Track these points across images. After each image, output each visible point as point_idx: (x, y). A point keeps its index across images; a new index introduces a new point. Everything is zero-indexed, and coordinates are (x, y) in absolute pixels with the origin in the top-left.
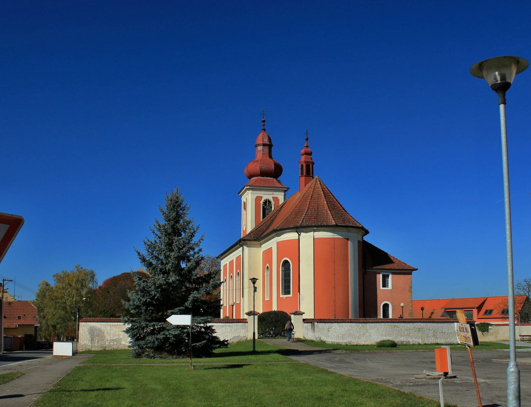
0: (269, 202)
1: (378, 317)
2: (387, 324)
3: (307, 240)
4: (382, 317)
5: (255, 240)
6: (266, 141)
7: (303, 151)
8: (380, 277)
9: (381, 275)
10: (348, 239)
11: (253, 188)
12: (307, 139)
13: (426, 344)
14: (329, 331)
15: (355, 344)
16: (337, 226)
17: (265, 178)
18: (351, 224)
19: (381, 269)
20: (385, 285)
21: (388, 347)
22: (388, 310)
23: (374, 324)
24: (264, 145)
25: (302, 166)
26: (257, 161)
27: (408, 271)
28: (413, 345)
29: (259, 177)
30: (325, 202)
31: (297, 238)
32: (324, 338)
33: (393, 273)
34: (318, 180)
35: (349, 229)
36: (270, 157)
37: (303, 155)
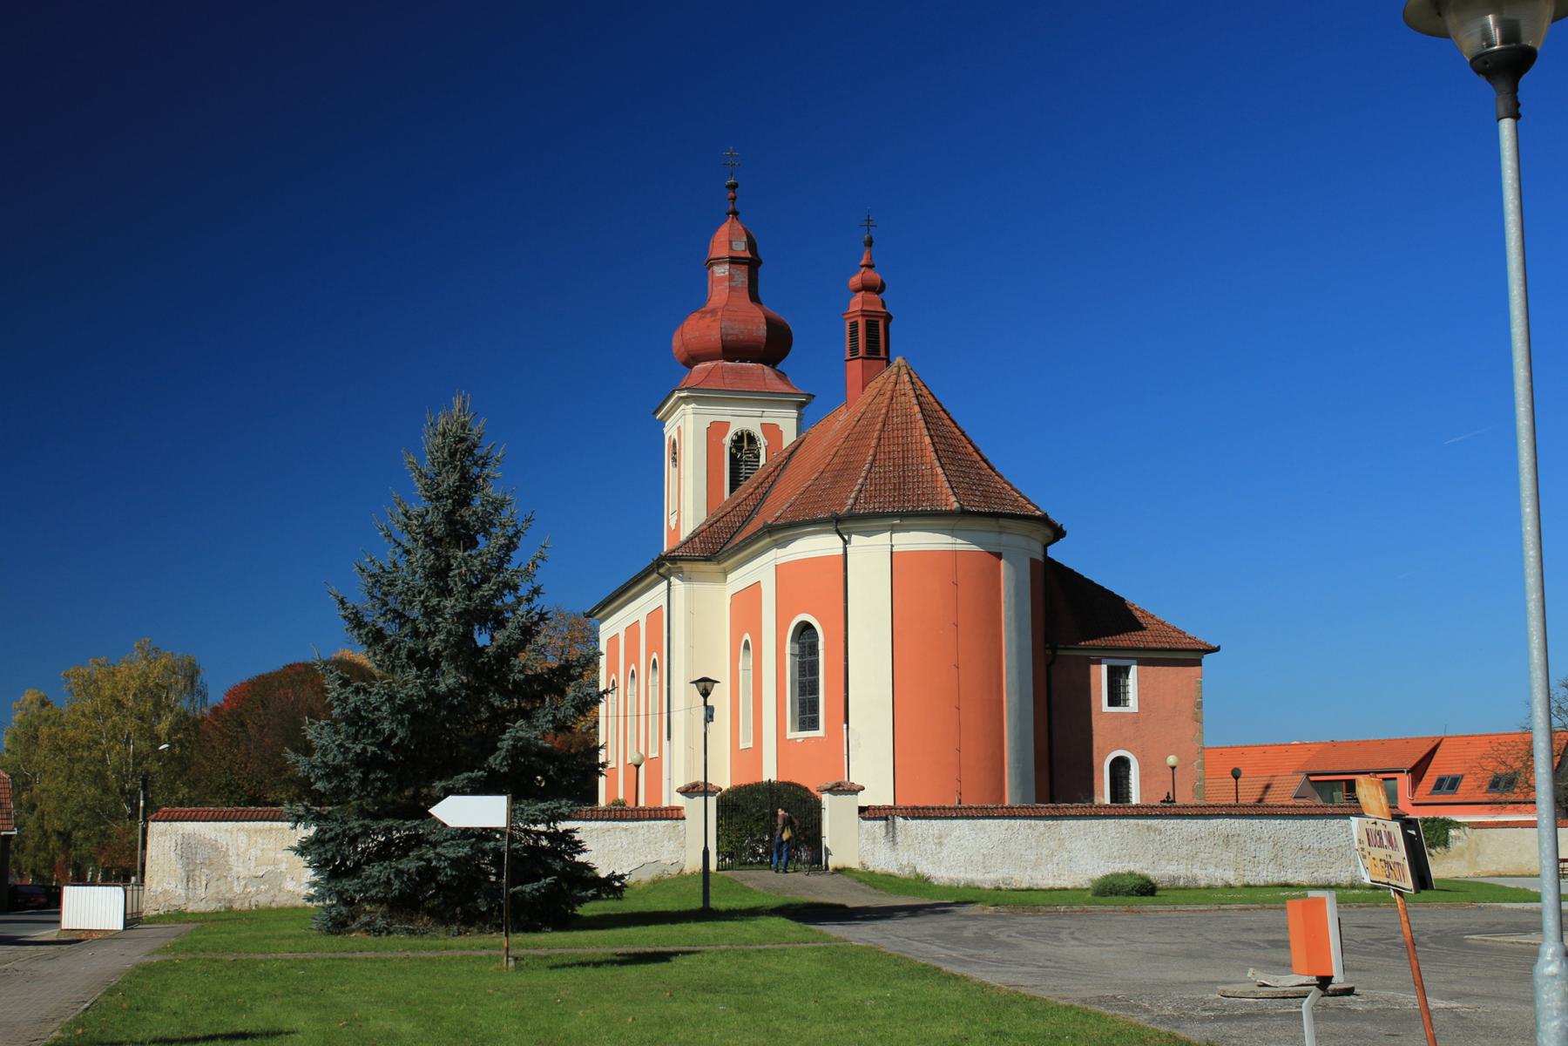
0: (752, 439)
1: (1097, 802)
2: (1124, 821)
3: (871, 558)
4: (1107, 801)
5: (707, 559)
7: (855, 280)
8: (1100, 675)
9: (1104, 668)
10: (999, 556)
11: (703, 395)
12: (870, 243)
13: (1248, 886)
14: (941, 844)
15: (1024, 886)
16: (963, 513)
17: (737, 364)
18: (1008, 509)
19: (1104, 649)
20: (1116, 697)
21: (1128, 894)
22: (1127, 777)
23: (1082, 822)
24: (734, 261)
25: (854, 325)
26: (713, 312)
27: (1189, 655)
28: (1209, 887)
29: (720, 363)
30: (927, 440)
31: (841, 552)
32: (925, 868)
33: (1141, 662)
34: (903, 370)
35: (1002, 522)
36: (754, 297)
37: (857, 291)
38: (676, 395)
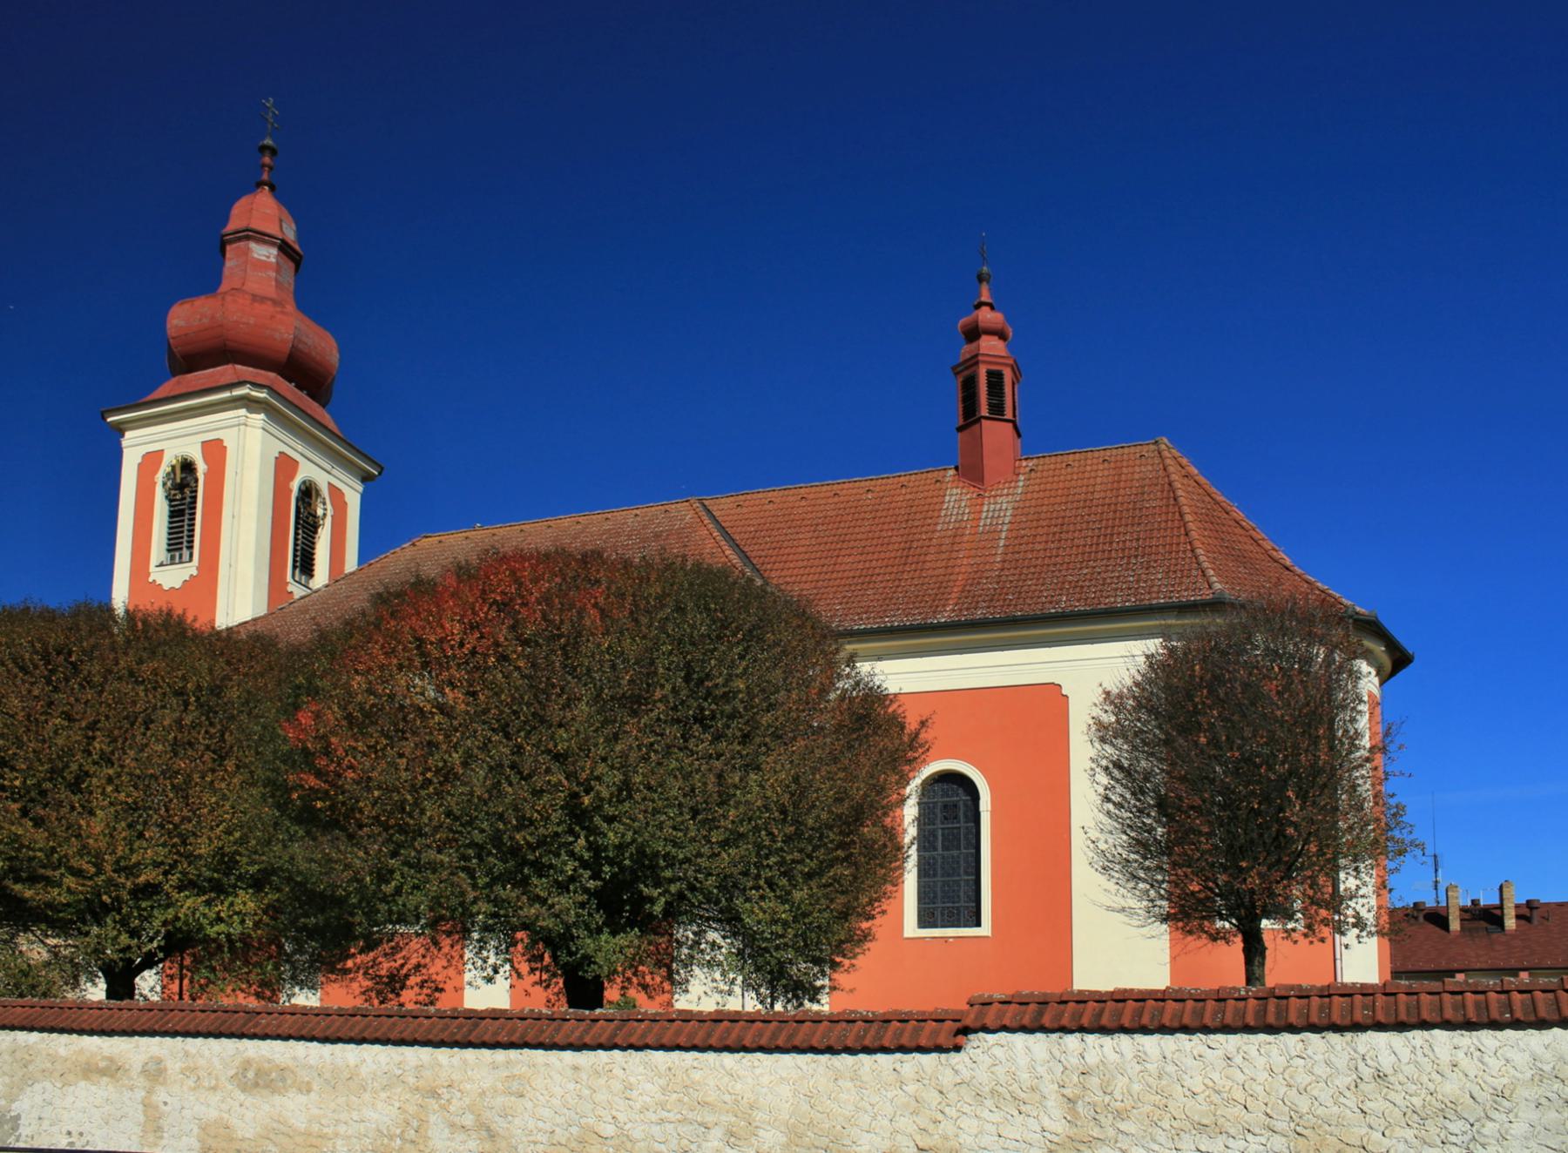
0: (318, 493)
6: (290, 234)
38: (238, 392)
